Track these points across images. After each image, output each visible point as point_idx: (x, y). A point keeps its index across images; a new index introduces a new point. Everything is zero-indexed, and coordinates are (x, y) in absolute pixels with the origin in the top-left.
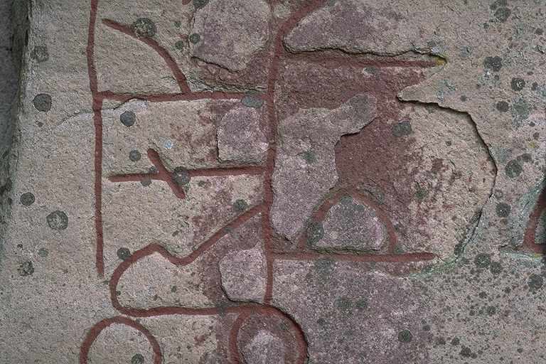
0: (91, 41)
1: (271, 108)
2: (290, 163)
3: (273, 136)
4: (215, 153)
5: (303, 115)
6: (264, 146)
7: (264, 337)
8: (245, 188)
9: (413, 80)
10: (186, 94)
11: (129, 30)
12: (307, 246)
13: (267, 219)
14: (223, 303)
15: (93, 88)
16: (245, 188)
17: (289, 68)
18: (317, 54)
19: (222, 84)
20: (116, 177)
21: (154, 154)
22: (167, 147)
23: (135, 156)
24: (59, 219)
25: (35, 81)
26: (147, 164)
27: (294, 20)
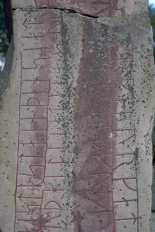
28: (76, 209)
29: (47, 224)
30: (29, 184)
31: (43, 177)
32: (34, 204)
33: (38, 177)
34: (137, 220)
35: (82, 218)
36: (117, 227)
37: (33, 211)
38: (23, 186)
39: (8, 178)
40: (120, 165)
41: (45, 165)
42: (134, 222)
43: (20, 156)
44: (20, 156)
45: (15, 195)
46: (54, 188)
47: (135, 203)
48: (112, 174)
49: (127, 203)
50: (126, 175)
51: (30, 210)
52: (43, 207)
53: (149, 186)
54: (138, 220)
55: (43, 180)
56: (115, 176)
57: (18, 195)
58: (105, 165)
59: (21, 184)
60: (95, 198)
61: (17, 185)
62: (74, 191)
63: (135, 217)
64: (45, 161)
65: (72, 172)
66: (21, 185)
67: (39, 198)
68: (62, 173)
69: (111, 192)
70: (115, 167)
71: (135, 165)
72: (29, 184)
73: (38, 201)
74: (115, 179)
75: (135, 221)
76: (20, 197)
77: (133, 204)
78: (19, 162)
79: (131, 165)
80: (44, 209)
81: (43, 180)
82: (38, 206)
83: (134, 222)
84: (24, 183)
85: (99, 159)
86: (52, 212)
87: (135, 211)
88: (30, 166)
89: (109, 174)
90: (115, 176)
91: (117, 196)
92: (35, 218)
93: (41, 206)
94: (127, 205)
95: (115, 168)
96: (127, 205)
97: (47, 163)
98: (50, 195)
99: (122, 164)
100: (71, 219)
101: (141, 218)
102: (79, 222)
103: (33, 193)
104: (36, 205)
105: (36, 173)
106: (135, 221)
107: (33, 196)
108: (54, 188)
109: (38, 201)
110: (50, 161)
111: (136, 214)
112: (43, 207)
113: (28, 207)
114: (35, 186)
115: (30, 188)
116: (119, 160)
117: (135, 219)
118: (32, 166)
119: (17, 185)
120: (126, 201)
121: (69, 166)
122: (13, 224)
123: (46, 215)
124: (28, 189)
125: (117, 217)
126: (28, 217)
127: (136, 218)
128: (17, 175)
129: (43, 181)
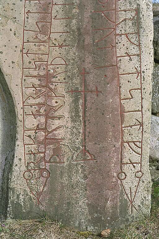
0: (23, 138)
1: (45, 146)
2: (48, 152)
3: (45, 149)
4: (39, 151)
5: (49, 146)
6: (44, 150)
7: (45, 172)
8: (42, 155)
9: (62, 141)
10: (35, 144)
11: (28, 136)
12: (49, 162)
13: (45, 158)
14: (40, 169)
15: (24, 144)
16: (42, 155)
17: (47, 141)
18: (51, 139)
19: (39, 143)
20: (26, 154)
21: (31, 151)
22: (33, 150)
23: (29, 151)
24: (20, 159)
25: (18, 143)
26: (30, 152)
27: (48, 135)
30: (35, 40)
31: (49, 33)
32: (41, 60)
34: (140, 74)
36: (122, 81)
38: (30, 42)
39: (15, 34)
40: (123, 21)
41: (51, 21)
42: (138, 77)
43: (27, 13)
44: (27, 13)
45: (22, 51)
46: (60, 44)
48: (115, 29)
49: (130, 58)
50: (128, 31)
51: (37, 66)
52: (49, 63)
53: (151, 41)
54: (141, 74)
55: (49, 36)
56: (118, 32)
57: (25, 51)
58: (109, 21)
59: (28, 41)
61: (23, 41)
63: (131, 162)
64: (51, 18)
66: (28, 41)
67: (45, 54)
69: (115, 47)
70: (118, 23)
72: (35, 40)
73: (45, 57)
74: (118, 35)
75: (138, 75)
77: (135, 59)
78: (26, 18)
80: (50, 65)
81: (49, 36)
82: (44, 62)
83: (138, 77)
84: (31, 40)
85: (103, 15)
86: (58, 68)
87: (137, 65)
88: (36, 23)
89: (113, 30)
90: (118, 32)
91: (120, 51)
92: (42, 73)
93: (47, 62)
94: (131, 60)
95: (118, 24)
96: (131, 60)
97: (52, 19)
99: (125, 20)
101: (144, 72)
102: (85, 77)
104: (43, 61)
105: (42, 29)
106: (138, 75)
107: (39, 52)
108: (60, 45)
109: (45, 57)
110: (55, 17)
111: (139, 69)
112: (49, 63)
113: (35, 63)
114: (41, 42)
115: (37, 44)
116: (122, 16)
117: (138, 73)
118: (38, 22)
119: (23, 41)
122: (20, 81)
123: (52, 71)
124: (35, 45)
125: (121, 71)
126: (35, 73)
127: (139, 73)
128: (24, 31)
129: (49, 37)
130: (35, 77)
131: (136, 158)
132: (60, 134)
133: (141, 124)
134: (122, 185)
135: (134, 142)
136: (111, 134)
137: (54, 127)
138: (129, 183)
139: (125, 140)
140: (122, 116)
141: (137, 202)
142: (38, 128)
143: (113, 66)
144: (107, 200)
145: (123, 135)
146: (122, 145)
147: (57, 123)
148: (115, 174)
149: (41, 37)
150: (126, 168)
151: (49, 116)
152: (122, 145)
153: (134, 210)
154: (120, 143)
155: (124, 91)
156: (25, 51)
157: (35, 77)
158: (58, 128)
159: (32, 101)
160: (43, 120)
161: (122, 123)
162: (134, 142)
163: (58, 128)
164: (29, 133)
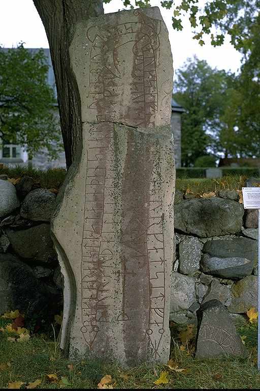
2: (98, 314)
8: (94, 316)
28: (123, 254)
29: (103, 265)
32: (94, 250)
33: (98, 233)
35: (127, 261)
36: (150, 267)
37: (94, 255)
47: (162, 250)
48: (147, 231)
56: (149, 233)
57: (84, 245)
60: (135, 247)
62: (121, 242)
65: (120, 230)
68: (113, 230)
71: (162, 224)
76: (85, 246)
79: (160, 225)
92: (95, 260)
94: (157, 252)
96: (157, 252)
98: (105, 245)
99: (154, 224)
100: (119, 261)
103: (94, 244)
116: (152, 221)
120: (156, 249)
121: (118, 225)
122: (80, 264)
125: (150, 260)
126: (91, 260)
130: (91, 262)
131: (160, 319)
132: (108, 302)
133: (164, 296)
134: (149, 338)
135: (158, 309)
136: (142, 302)
137: (103, 297)
138: (155, 336)
139: (152, 307)
140: (151, 291)
141: (160, 351)
142: (91, 298)
143: (145, 256)
144: (138, 348)
145: (150, 304)
146: (150, 310)
147: (104, 294)
148: (145, 331)
149: (95, 235)
150: (153, 327)
151: (100, 289)
152: (150, 310)
153: (157, 355)
154: (148, 309)
155: (153, 274)
156: (84, 245)
157: (91, 262)
158: (106, 298)
159: (87, 279)
160: (95, 292)
161: (150, 295)
162: (158, 309)
163: (106, 298)
164: (85, 301)
